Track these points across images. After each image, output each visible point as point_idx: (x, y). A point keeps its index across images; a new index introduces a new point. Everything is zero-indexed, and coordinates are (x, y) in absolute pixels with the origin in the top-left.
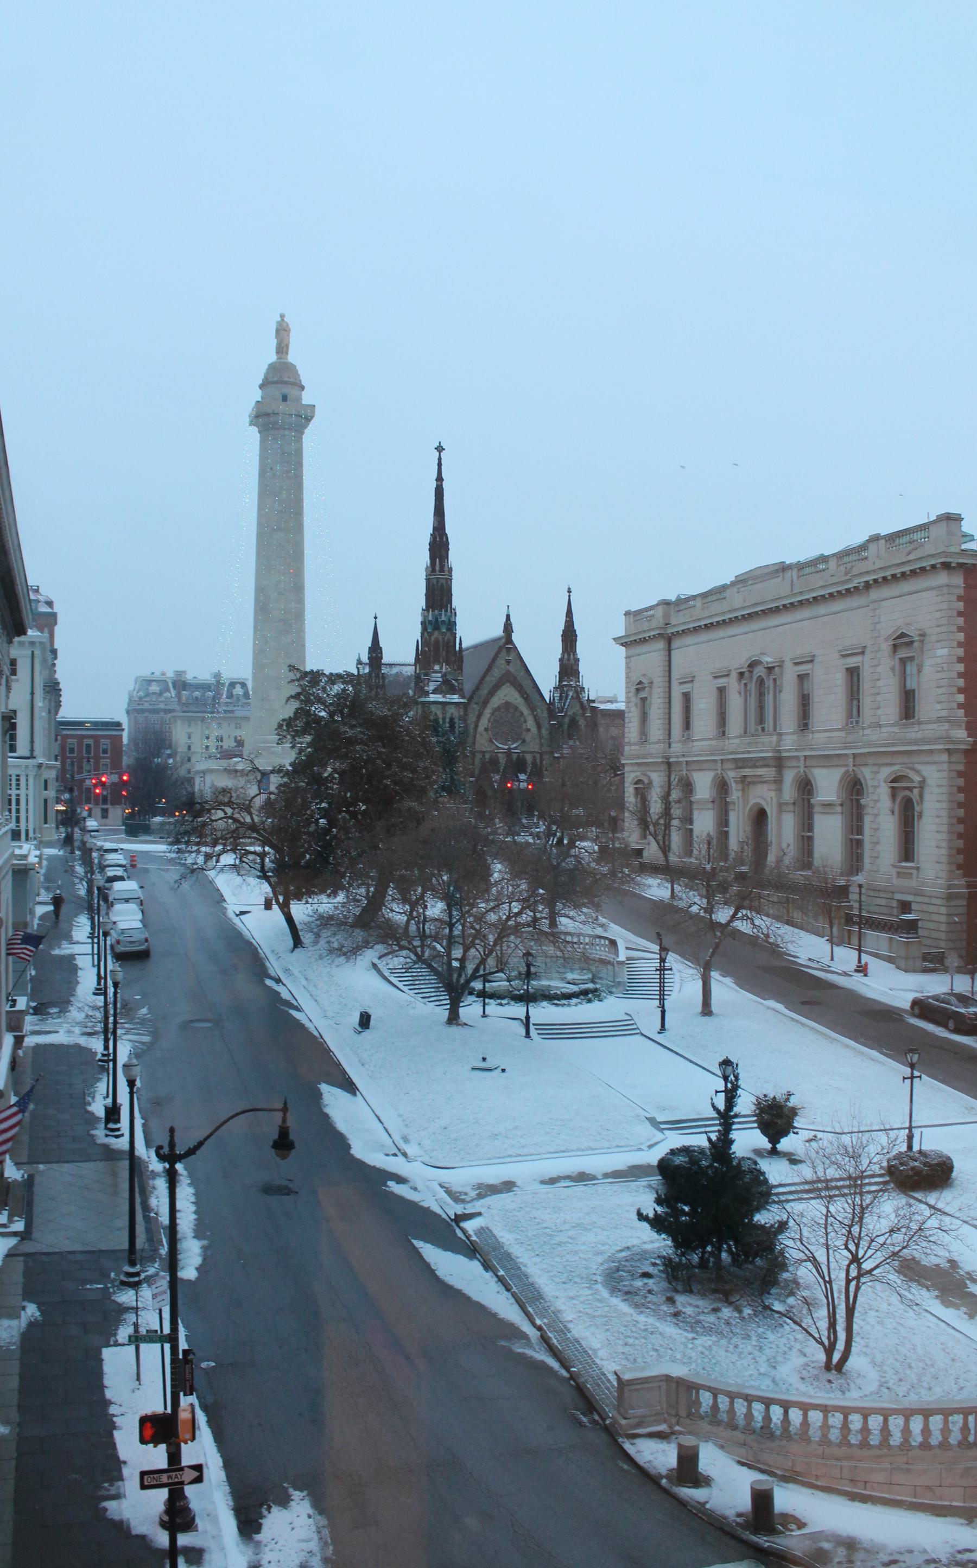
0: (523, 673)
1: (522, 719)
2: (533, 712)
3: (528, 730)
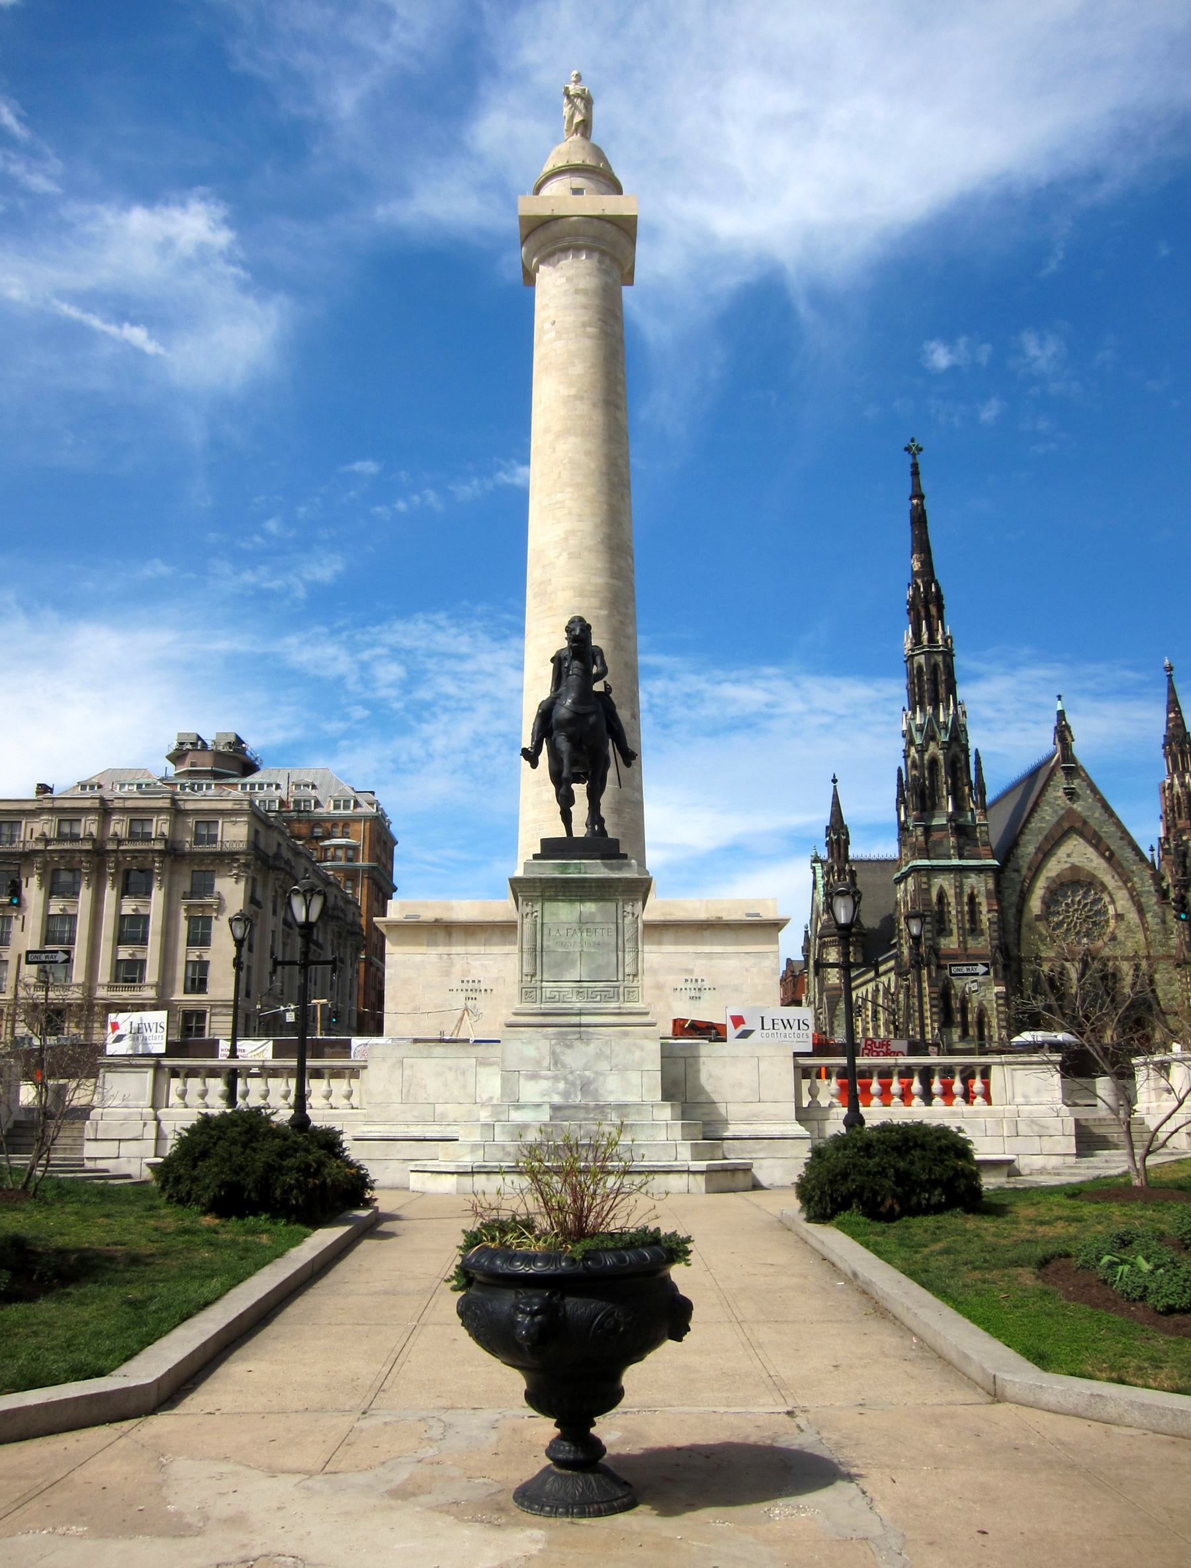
0: (1098, 812)
1: (1106, 899)
2: (1125, 882)
3: (1119, 917)
